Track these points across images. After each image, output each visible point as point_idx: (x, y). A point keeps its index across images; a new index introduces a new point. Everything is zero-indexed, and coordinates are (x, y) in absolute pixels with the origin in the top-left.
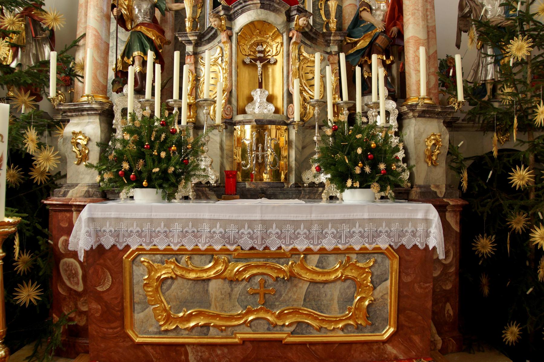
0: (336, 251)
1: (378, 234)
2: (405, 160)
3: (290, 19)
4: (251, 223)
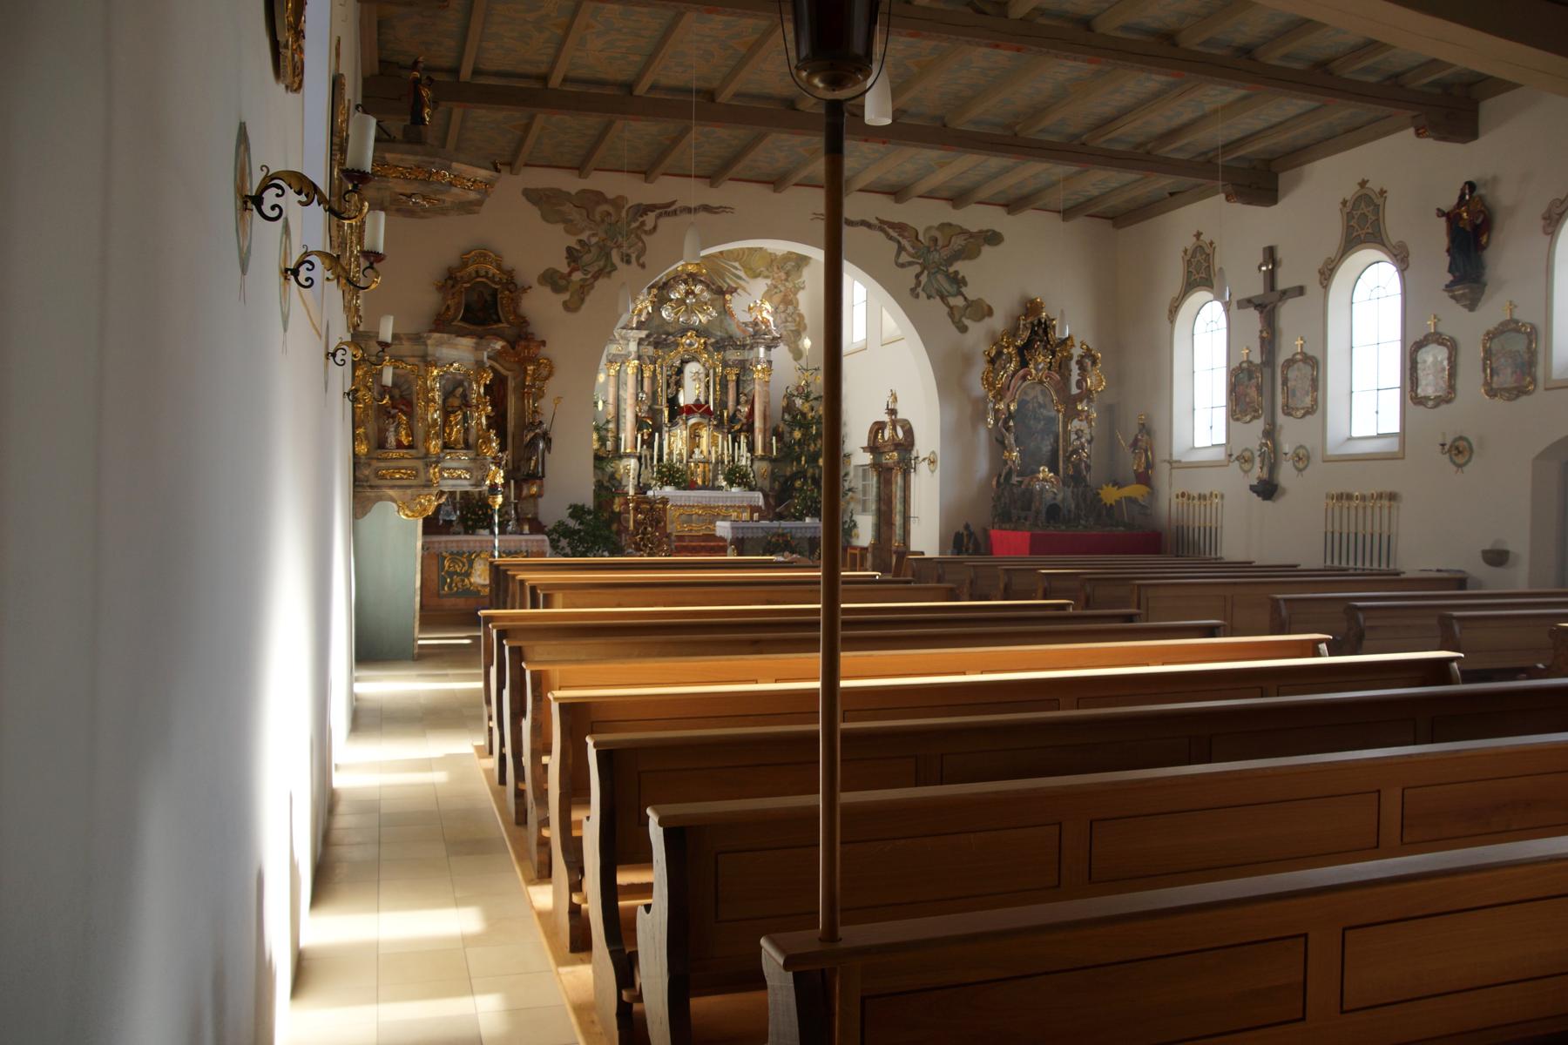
0: (731, 506)
1: (743, 501)
2: (754, 477)
3: (710, 420)
4: (706, 497)
